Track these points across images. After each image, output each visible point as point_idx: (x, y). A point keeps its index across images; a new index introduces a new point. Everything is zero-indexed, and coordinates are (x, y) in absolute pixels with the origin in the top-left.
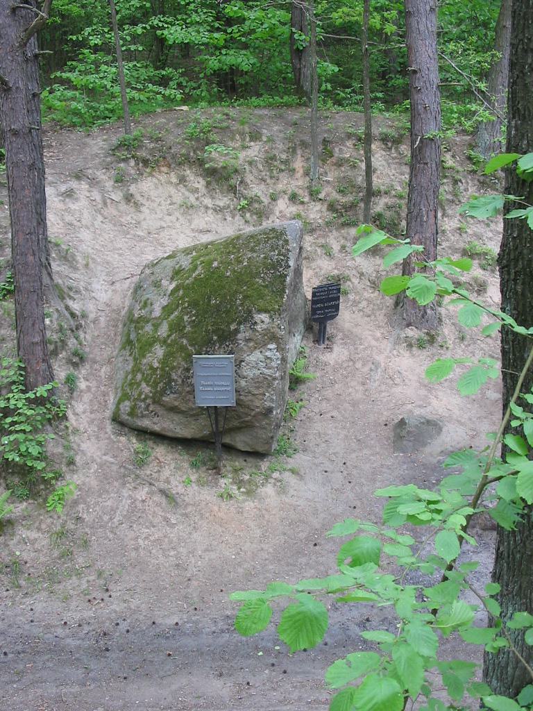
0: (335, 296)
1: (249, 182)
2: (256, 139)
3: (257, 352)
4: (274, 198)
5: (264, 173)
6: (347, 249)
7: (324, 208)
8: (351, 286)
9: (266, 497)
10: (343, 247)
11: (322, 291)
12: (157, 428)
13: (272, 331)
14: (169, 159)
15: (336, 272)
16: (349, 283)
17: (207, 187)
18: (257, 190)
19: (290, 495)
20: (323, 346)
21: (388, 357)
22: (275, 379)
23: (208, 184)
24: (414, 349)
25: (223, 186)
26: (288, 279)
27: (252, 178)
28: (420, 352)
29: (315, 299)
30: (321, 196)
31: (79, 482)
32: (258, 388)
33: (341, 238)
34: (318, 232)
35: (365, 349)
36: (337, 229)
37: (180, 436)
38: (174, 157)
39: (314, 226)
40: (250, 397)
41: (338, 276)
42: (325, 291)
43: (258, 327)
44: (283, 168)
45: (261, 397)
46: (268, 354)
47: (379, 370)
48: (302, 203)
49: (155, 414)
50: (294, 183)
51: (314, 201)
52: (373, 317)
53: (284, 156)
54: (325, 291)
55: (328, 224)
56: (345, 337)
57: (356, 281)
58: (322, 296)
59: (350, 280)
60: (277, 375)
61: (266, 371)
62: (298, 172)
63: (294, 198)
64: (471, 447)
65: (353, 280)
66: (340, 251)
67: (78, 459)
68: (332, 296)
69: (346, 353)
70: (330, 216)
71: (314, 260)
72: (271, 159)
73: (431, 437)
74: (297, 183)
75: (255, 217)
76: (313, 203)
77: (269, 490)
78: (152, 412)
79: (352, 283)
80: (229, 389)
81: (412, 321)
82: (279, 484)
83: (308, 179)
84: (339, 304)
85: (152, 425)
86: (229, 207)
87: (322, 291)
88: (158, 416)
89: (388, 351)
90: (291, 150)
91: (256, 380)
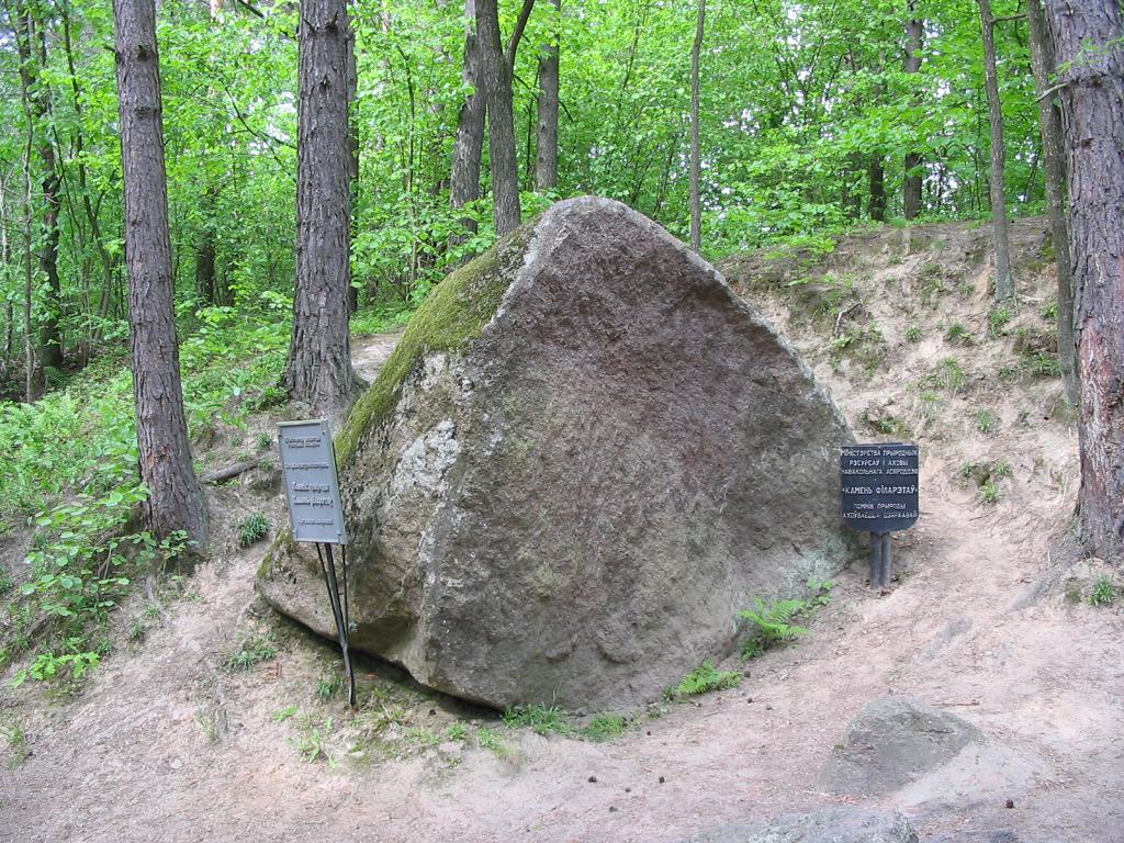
0: (905, 472)
1: (875, 313)
2: (920, 249)
3: (420, 440)
4: (914, 338)
5: (909, 299)
6: (1028, 419)
7: (1008, 350)
8: (1010, 488)
9: (386, 781)
10: (1023, 416)
11: (865, 457)
12: (289, 606)
13: (445, 388)
14: (741, 282)
15: (985, 460)
16: (1006, 481)
17: (791, 321)
18: (888, 327)
19: (444, 791)
20: (880, 589)
21: (1005, 617)
22: (435, 497)
23: (794, 315)
24: (1082, 606)
25: (821, 320)
26: (512, 286)
27: (886, 307)
28: (1093, 613)
29: (849, 472)
30: (1006, 328)
31: (126, 671)
32: (409, 518)
33: (1024, 400)
34: (978, 392)
35: (959, 598)
36: (1021, 385)
37: (321, 629)
38: (748, 279)
39: (972, 380)
40: (396, 539)
41: (986, 467)
42: (873, 458)
43: (425, 385)
44: (949, 286)
45: (414, 540)
46: (434, 441)
47: (959, 638)
48: (969, 344)
49: (291, 576)
50: (964, 311)
51: (993, 339)
52: (1025, 545)
53: (956, 268)
54: (873, 458)
55: (1005, 375)
56: (938, 575)
57: (1022, 478)
58: (867, 467)
59: (1010, 475)
60: (441, 488)
61: (424, 480)
62: (978, 293)
63: (953, 335)
64: (1010, 805)
65: (1017, 476)
66: (1015, 425)
67: (154, 638)
68: (896, 471)
69: (914, 602)
70: (1013, 360)
71: (951, 440)
72: (931, 272)
73: (923, 766)
74: (970, 313)
75: (860, 367)
76: (991, 343)
77: (410, 770)
78: (286, 570)
79: (1014, 481)
80: (328, 498)
81: (1097, 546)
82: (440, 764)
83: (992, 301)
84: (916, 493)
85: (284, 598)
86: (815, 350)
87: (865, 457)
88: (294, 583)
89: (1009, 605)
90: (972, 256)
91: (406, 499)
